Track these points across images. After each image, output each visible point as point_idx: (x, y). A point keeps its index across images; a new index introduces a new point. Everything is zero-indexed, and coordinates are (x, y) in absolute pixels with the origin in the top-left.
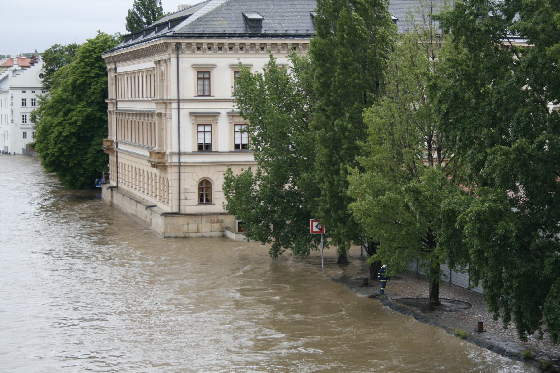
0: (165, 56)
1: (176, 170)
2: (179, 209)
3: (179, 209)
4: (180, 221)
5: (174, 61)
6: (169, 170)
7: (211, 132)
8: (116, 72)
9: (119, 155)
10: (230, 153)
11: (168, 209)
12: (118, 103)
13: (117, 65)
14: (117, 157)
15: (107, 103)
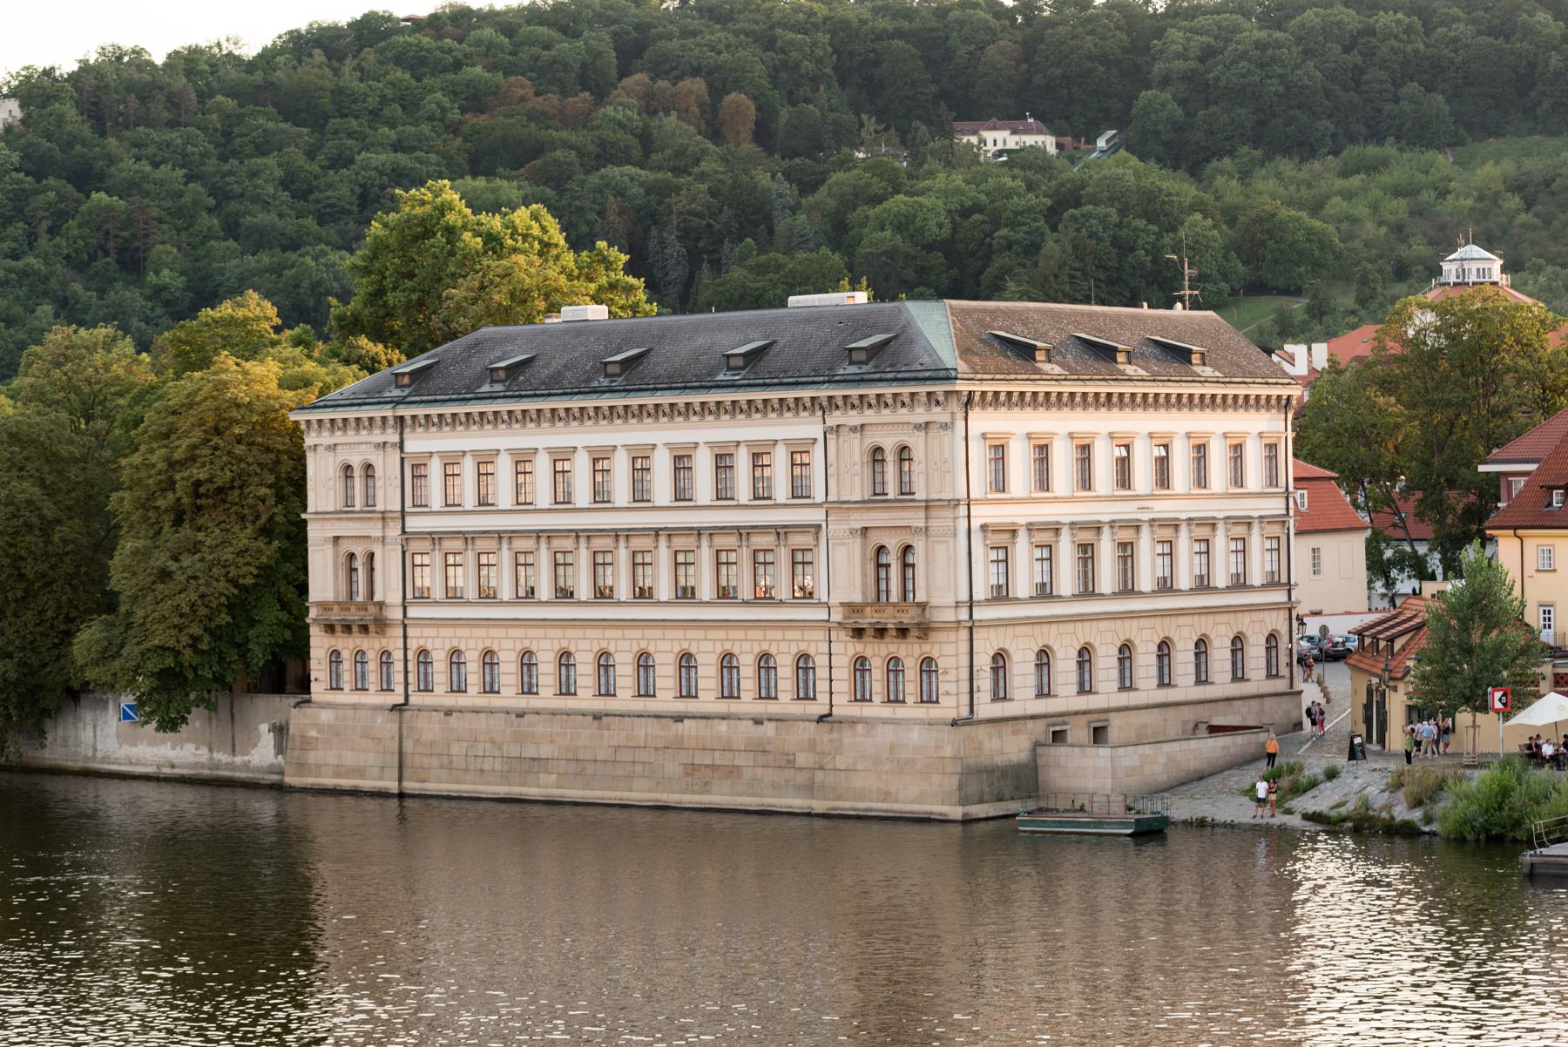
0: (939, 415)
1: (964, 634)
2: (972, 711)
3: (972, 711)
4: (981, 732)
5: (960, 424)
6: (935, 636)
7: (1050, 559)
8: (402, 450)
9: (410, 632)
10: (1032, 599)
11: (952, 714)
12: (407, 519)
13: (406, 436)
14: (405, 637)
15: (305, 521)
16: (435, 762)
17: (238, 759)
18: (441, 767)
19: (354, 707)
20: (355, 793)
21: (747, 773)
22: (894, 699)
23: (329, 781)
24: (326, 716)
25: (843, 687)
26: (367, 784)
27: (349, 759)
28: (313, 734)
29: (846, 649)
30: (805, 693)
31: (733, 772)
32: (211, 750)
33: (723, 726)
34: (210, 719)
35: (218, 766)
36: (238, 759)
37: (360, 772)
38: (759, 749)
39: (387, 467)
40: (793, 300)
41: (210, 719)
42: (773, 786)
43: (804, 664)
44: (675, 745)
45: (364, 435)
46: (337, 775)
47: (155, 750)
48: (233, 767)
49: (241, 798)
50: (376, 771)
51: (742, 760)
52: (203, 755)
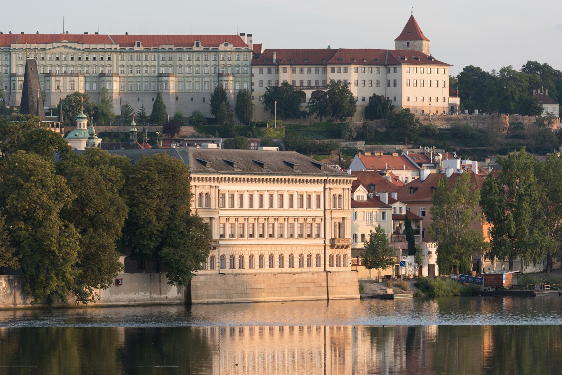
16: (233, 291)
17: (162, 296)
18: (235, 293)
19: (211, 275)
20: (214, 303)
21: (312, 289)
22: (338, 265)
23: (206, 300)
24: (202, 278)
25: (327, 263)
26: (217, 300)
27: (211, 292)
28: (199, 284)
29: (329, 251)
30: (318, 265)
31: (308, 289)
32: (151, 294)
33: (305, 275)
34: (151, 282)
35: (154, 299)
36: (162, 296)
37: (214, 297)
38: (314, 282)
39: (214, 194)
40: (265, 148)
41: (151, 282)
42: (318, 292)
43: (318, 256)
44: (294, 282)
45: (209, 184)
46: (208, 298)
47: (127, 296)
48: (160, 299)
49: (163, 309)
50: (219, 296)
51: (310, 285)
52: (148, 296)
